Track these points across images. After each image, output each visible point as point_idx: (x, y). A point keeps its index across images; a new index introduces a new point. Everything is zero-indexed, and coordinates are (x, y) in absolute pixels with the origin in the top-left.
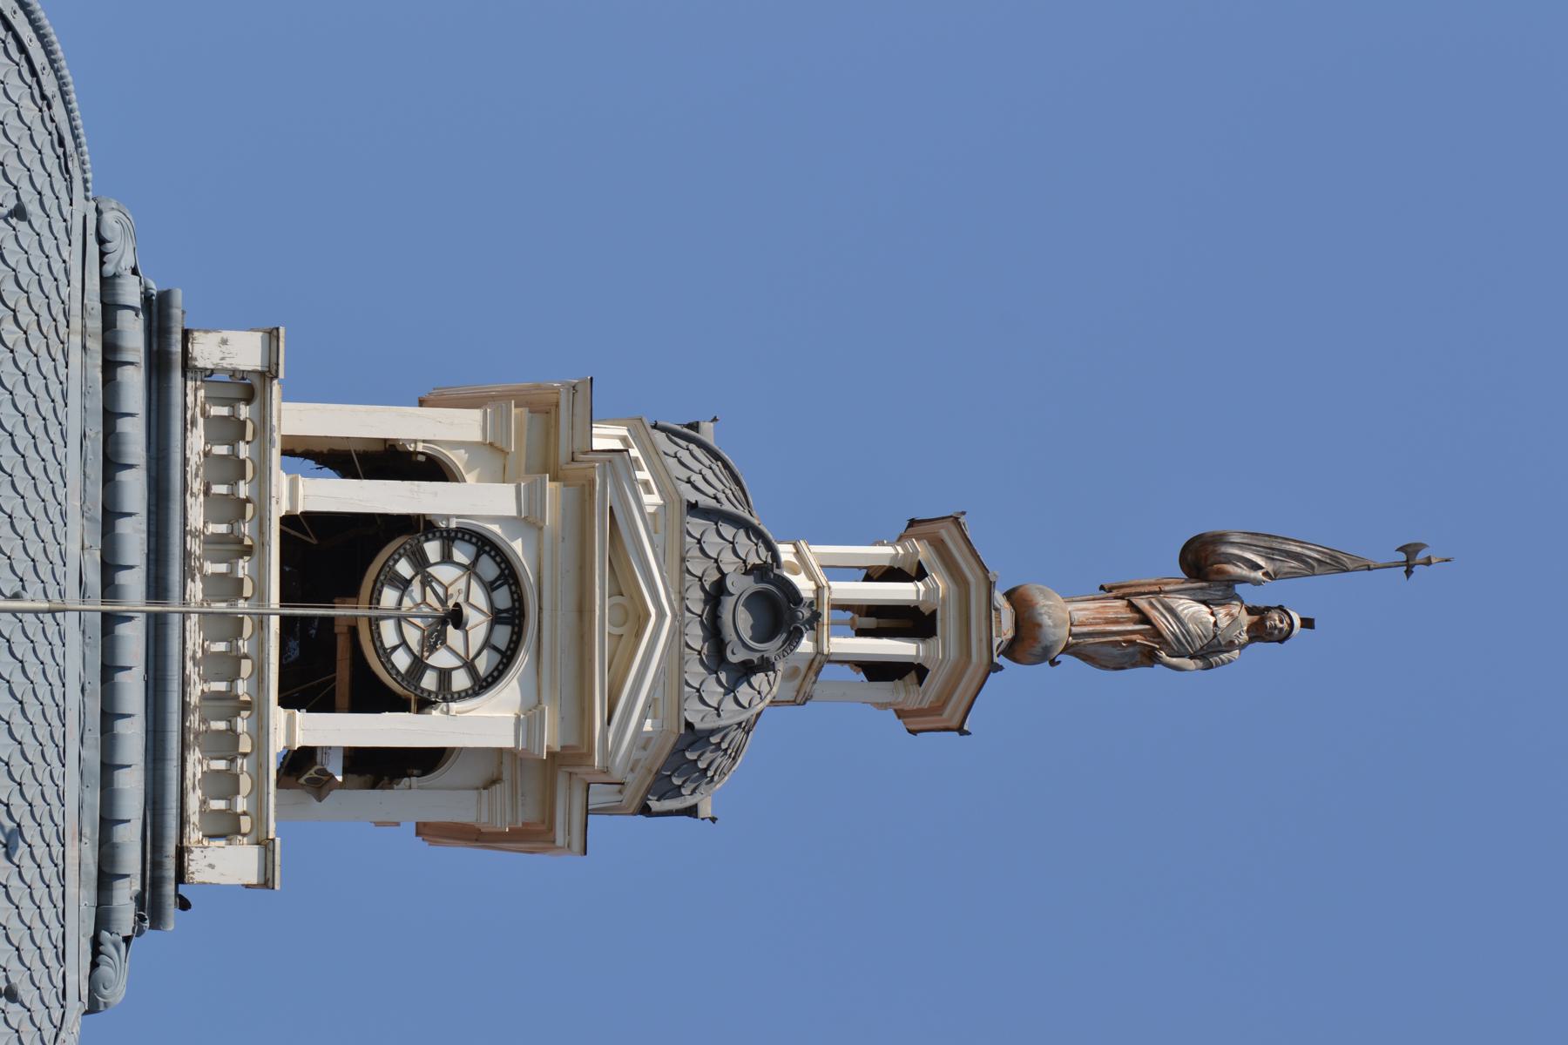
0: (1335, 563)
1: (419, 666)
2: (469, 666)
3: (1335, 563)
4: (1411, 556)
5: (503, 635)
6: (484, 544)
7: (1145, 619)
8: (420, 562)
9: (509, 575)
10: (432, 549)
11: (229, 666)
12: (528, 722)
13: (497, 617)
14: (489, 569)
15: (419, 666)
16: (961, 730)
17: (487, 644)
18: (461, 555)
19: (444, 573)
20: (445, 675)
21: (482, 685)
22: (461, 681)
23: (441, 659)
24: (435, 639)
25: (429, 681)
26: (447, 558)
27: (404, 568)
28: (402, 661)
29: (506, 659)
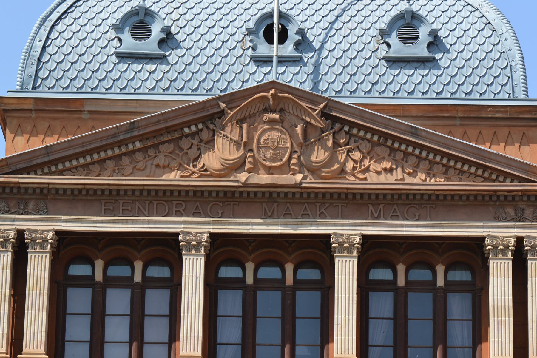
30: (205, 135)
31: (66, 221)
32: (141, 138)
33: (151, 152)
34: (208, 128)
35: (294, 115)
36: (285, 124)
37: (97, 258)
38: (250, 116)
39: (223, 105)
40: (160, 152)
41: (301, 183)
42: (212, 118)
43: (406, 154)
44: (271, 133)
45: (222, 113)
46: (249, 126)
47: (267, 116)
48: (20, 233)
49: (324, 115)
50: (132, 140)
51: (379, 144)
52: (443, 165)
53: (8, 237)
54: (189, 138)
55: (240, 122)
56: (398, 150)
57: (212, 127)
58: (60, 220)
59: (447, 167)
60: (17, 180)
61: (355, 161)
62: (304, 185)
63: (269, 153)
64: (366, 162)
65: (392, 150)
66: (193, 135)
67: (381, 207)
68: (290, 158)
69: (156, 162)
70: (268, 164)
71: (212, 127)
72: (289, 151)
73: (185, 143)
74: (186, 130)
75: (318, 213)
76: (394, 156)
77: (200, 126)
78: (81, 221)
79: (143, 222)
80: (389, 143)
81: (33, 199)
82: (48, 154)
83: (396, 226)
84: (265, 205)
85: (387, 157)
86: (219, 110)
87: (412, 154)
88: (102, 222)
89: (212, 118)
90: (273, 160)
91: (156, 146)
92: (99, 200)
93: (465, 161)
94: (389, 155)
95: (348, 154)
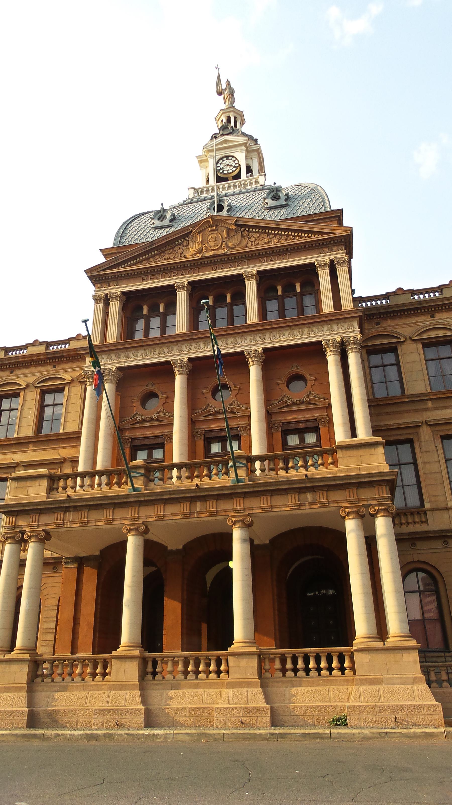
0: (219, 77)
1: (235, 167)
2: (234, 161)
3: (219, 77)
4: (217, 68)
5: (230, 158)
6: (218, 162)
7: (228, 96)
8: (220, 169)
9: (222, 159)
10: (218, 168)
11: (235, 186)
12: (241, 151)
13: (227, 159)
14: (221, 161)
15: (235, 167)
16: (243, 112)
17: (231, 160)
18: (219, 165)
19: (222, 166)
20: (236, 164)
21: (237, 159)
22: (236, 162)
23: (233, 165)
24: (231, 165)
25: (237, 165)
26: (220, 166)
27: (221, 171)
28: (234, 169)
29: (233, 157)
30: (185, 243)
31: (126, 287)
32: (157, 248)
33: (162, 254)
34: (186, 240)
35: (222, 227)
36: (219, 231)
37: (144, 305)
38: (203, 230)
39: (191, 229)
40: (166, 254)
41: (227, 252)
42: (187, 235)
43: (275, 235)
44: (212, 235)
45: (191, 232)
46: (202, 235)
47: (210, 229)
48: (106, 295)
49: (236, 225)
50: (153, 249)
51: (262, 233)
52: (293, 236)
53: (101, 297)
54: (178, 246)
55: (199, 233)
56: (271, 233)
57: (187, 239)
58: (123, 287)
59: (294, 236)
60: (104, 273)
61: (252, 242)
62: (228, 253)
63: (212, 244)
64: (257, 242)
65: (269, 234)
66: (180, 244)
67: (265, 258)
68: (222, 244)
69: (164, 258)
70: (213, 249)
71: (187, 239)
72: (221, 241)
73: (176, 249)
74: (177, 243)
75: (237, 265)
76: (270, 237)
77: (183, 240)
78: (132, 286)
79: (159, 282)
80: (267, 231)
81: (112, 281)
82: (116, 260)
83: (272, 264)
84: (212, 266)
85: (266, 238)
86: (189, 231)
87: (278, 234)
88: (141, 285)
89: (187, 235)
90: (215, 246)
91: (164, 252)
92: (140, 277)
93: (302, 231)
94: (267, 237)
95: (248, 240)
